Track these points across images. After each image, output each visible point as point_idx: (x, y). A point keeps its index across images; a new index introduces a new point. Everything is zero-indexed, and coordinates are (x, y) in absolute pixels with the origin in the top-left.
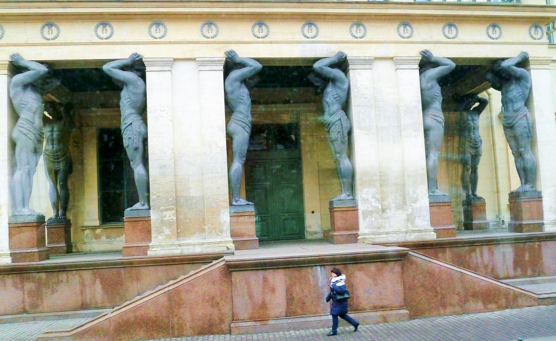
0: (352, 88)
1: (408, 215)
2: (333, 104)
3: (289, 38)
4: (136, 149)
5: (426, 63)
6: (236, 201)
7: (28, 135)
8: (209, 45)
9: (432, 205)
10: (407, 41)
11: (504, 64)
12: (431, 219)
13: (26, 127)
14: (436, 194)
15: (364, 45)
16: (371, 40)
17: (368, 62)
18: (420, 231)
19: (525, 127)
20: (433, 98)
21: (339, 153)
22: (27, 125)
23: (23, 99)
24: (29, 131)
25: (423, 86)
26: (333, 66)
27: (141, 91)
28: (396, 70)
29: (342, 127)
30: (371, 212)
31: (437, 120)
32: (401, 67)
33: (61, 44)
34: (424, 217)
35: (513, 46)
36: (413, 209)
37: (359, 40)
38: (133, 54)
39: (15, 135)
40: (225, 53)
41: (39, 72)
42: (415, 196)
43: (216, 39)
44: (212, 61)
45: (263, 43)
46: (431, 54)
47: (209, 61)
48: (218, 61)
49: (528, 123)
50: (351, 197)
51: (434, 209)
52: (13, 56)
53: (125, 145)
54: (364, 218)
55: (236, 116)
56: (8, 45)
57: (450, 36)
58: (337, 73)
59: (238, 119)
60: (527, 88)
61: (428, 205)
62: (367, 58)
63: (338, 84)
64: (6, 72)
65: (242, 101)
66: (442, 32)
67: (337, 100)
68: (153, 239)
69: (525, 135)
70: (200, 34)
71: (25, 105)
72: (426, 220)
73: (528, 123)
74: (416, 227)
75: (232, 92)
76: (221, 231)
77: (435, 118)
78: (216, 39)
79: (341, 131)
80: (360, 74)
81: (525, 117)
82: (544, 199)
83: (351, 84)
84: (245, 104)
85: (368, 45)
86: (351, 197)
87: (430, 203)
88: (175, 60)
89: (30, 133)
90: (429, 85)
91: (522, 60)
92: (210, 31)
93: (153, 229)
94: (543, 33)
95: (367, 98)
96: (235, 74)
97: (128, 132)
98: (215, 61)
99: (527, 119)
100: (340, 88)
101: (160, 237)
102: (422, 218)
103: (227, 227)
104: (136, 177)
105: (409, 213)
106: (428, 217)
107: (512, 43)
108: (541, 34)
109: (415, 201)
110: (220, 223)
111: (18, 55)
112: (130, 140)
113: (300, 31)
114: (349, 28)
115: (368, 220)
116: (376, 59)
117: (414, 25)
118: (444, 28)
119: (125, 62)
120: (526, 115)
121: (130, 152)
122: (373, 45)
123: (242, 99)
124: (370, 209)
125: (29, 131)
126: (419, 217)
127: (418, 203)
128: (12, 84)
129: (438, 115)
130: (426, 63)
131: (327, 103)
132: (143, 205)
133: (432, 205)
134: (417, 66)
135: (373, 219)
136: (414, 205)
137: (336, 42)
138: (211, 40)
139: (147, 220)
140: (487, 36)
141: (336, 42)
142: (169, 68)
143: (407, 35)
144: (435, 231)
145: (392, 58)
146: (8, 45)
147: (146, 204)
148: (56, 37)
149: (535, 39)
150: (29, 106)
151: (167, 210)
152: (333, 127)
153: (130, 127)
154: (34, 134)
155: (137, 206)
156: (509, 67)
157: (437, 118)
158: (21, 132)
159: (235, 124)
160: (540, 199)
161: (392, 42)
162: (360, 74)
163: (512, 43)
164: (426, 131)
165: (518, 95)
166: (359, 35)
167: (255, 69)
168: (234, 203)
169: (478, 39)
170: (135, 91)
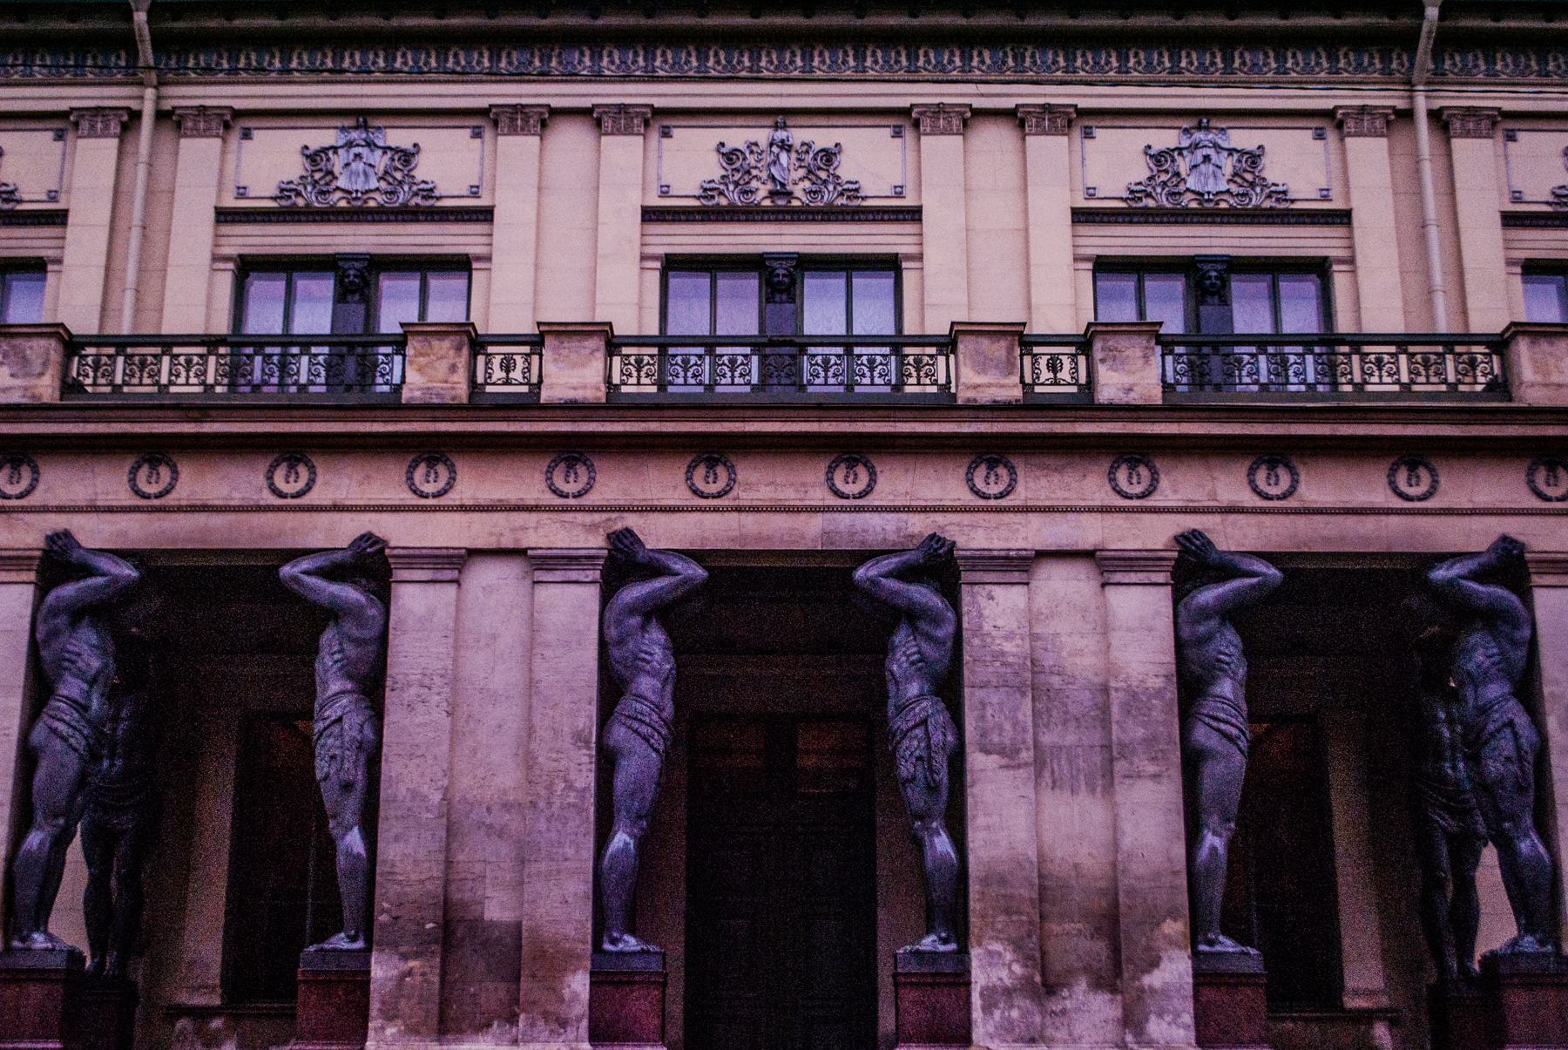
0: (966, 634)
2: (908, 680)
3: (790, 496)
4: (347, 787)
6: (614, 942)
7: (72, 741)
8: (568, 517)
13: (67, 718)
14: (1218, 948)
15: (1006, 518)
16: (1029, 503)
17: (1019, 566)
19: (1508, 759)
20: (1213, 670)
21: (921, 818)
22: (73, 716)
23: (71, 648)
24: (74, 728)
25: (1186, 632)
26: (907, 573)
27: (371, 633)
28: (1103, 585)
29: (928, 747)
30: (1008, 992)
32: (1118, 577)
33: (180, 509)
37: (993, 502)
38: (362, 537)
39: (39, 735)
40: (609, 536)
41: (116, 579)
43: (587, 500)
44: (570, 558)
45: (716, 510)
46: (1210, 542)
47: (563, 557)
48: (586, 557)
49: (1518, 748)
50: (952, 947)
51: (1209, 994)
52: (53, 539)
53: (319, 775)
54: (988, 1009)
55: (629, 705)
56: (45, 509)
57: (1273, 491)
58: (923, 595)
59: (632, 713)
60: (1515, 643)
62: (1012, 553)
63: (924, 626)
64: (32, 576)
65: (648, 667)
66: (1245, 480)
67: (920, 669)
68: (371, 1034)
69: (1509, 784)
70: (544, 486)
71: (73, 662)
72: (1186, 1027)
73: (1518, 748)
75: (621, 642)
76: (563, 1023)
77: (1215, 724)
78: (587, 500)
79: (924, 754)
80: (992, 598)
81: (1508, 731)
83: (965, 625)
84: (653, 674)
85: (1019, 518)
86: (952, 947)
87: (1195, 976)
88: (474, 553)
89: (77, 735)
92: (571, 479)
93: (375, 1006)
95: (1010, 665)
96: (634, 592)
97: (330, 741)
98: (577, 558)
99: (1516, 736)
100: (930, 638)
101: (391, 1031)
102: (1168, 1018)
103: (581, 1007)
104: (341, 861)
106: (1188, 1018)
107: (1473, 512)
110: (561, 1000)
111: (67, 534)
112: (332, 759)
113: (823, 478)
114: (962, 471)
115: (997, 1014)
116: (1043, 555)
119: (338, 556)
120: (1511, 724)
121: (329, 794)
122: (1035, 519)
123: (649, 662)
124: (1008, 982)
125: (74, 728)
126: (1160, 1015)
127: (1156, 972)
128: (44, 609)
129: (1222, 715)
131: (892, 673)
132: (353, 939)
135: (1015, 1014)
137: (924, 510)
138: (571, 501)
139: (362, 981)
140: (1389, 492)
141: (924, 510)
142: (454, 574)
143: (1138, 489)
145: (1088, 555)
146: (45, 509)
147: (361, 935)
148: (166, 492)
149: (1549, 499)
150: (80, 664)
151: (417, 955)
152: (906, 743)
153: (336, 729)
154: (86, 738)
155: (340, 942)
157: (1223, 726)
158: (54, 731)
159: (623, 729)
161: (1090, 510)
162: (992, 598)
163: (1473, 512)
165: (1487, 663)
166: (994, 489)
167: (685, 581)
168: (608, 946)
169: (1360, 498)
170: (356, 633)
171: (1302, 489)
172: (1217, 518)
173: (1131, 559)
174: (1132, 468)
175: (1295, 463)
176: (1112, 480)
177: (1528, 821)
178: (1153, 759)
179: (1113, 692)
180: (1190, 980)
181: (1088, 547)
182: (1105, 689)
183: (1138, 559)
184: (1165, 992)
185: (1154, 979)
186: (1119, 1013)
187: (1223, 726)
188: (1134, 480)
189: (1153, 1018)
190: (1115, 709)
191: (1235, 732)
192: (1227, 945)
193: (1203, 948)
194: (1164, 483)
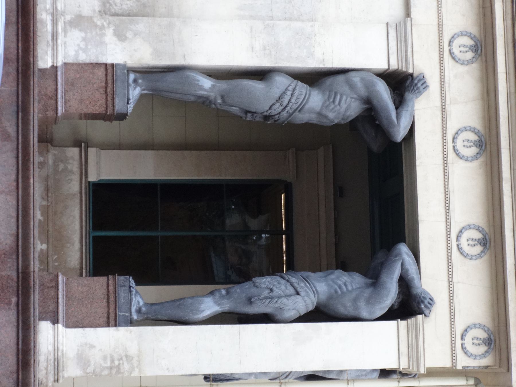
1: (91, 18)
5: (401, 84)
9: (110, 70)
10: (444, 50)
11: (404, 249)
12: (79, 64)
18: (55, 36)
19: (271, 290)
25: (356, 78)
31: (284, 93)
34: (85, 51)
35: (446, 284)
36: (102, 28)
42: (129, 35)
46: (420, 93)
49: (280, 297)
51: (100, 73)
57: (459, 144)
60: (355, 300)
61: (110, 60)
73: (280, 297)
74: (65, 31)
82: (112, 329)
87: (113, 65)
90: (359, 85)
91: (415, 295)
94: (475, 357)
102: (82, 45)
105: (95, 20)
106: (83, 58)
107: (450, 282)
108: (474, 357)
109: (121, 36)
117: (475, 66)
118: (473, 130)
126: (84, 39)
127: (115, 39)
129: (297, 93)
130: (401, 84)
133: (110, 69)
134: (394, 66)
136: (109, 32)
140: (463, 225)
143: (456, 51)
144: (54, 68)
145: (408, 14)
156: (399, 254)
157: (289, 93)
160: (112, 322)
163: (450, 282)
164: (261, 74)
165: (339, 282)
171: (462, 163)
172: (439, 104)
173: (406, 41)
174: (471, 48)
175: (481, 160)
176: (462, 34)
177: (227, 306)
178: (265, 48)
179: (311, 24)
180: (110, 61)
181: (413, 15)
182: (313, 20)
183: (406, 46)
184: (102, 43)
185: (109, 36)
186: (86, 11)
187: (289, 93)
188: (462, 49)
189: (83, 35)
190: (298, 24)
191: (285, 102)
192: (135, 93)
193: (132, 76)
194: (462, 69)
